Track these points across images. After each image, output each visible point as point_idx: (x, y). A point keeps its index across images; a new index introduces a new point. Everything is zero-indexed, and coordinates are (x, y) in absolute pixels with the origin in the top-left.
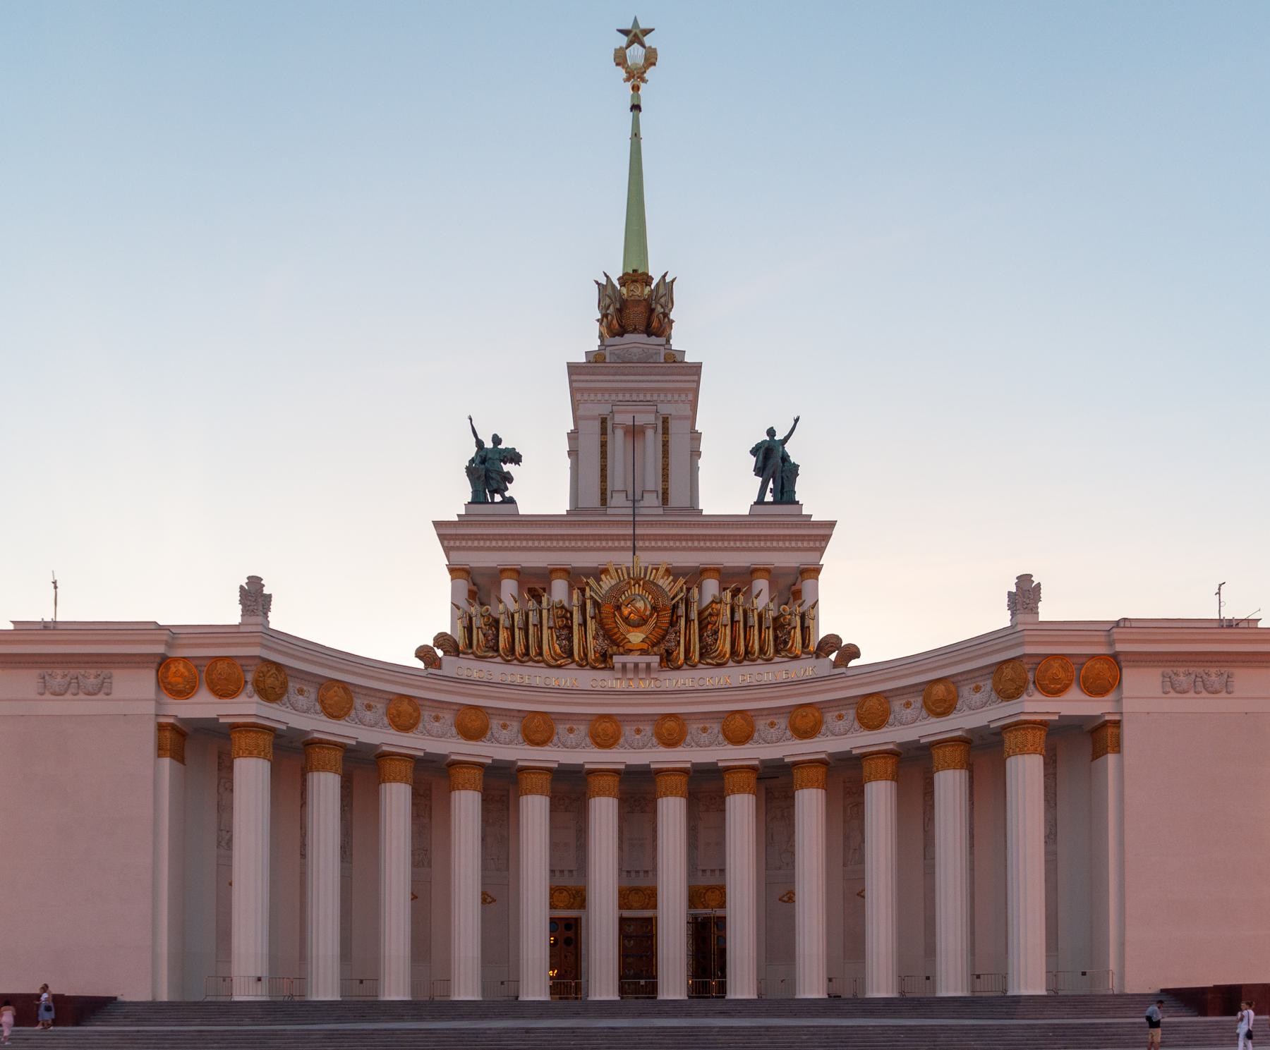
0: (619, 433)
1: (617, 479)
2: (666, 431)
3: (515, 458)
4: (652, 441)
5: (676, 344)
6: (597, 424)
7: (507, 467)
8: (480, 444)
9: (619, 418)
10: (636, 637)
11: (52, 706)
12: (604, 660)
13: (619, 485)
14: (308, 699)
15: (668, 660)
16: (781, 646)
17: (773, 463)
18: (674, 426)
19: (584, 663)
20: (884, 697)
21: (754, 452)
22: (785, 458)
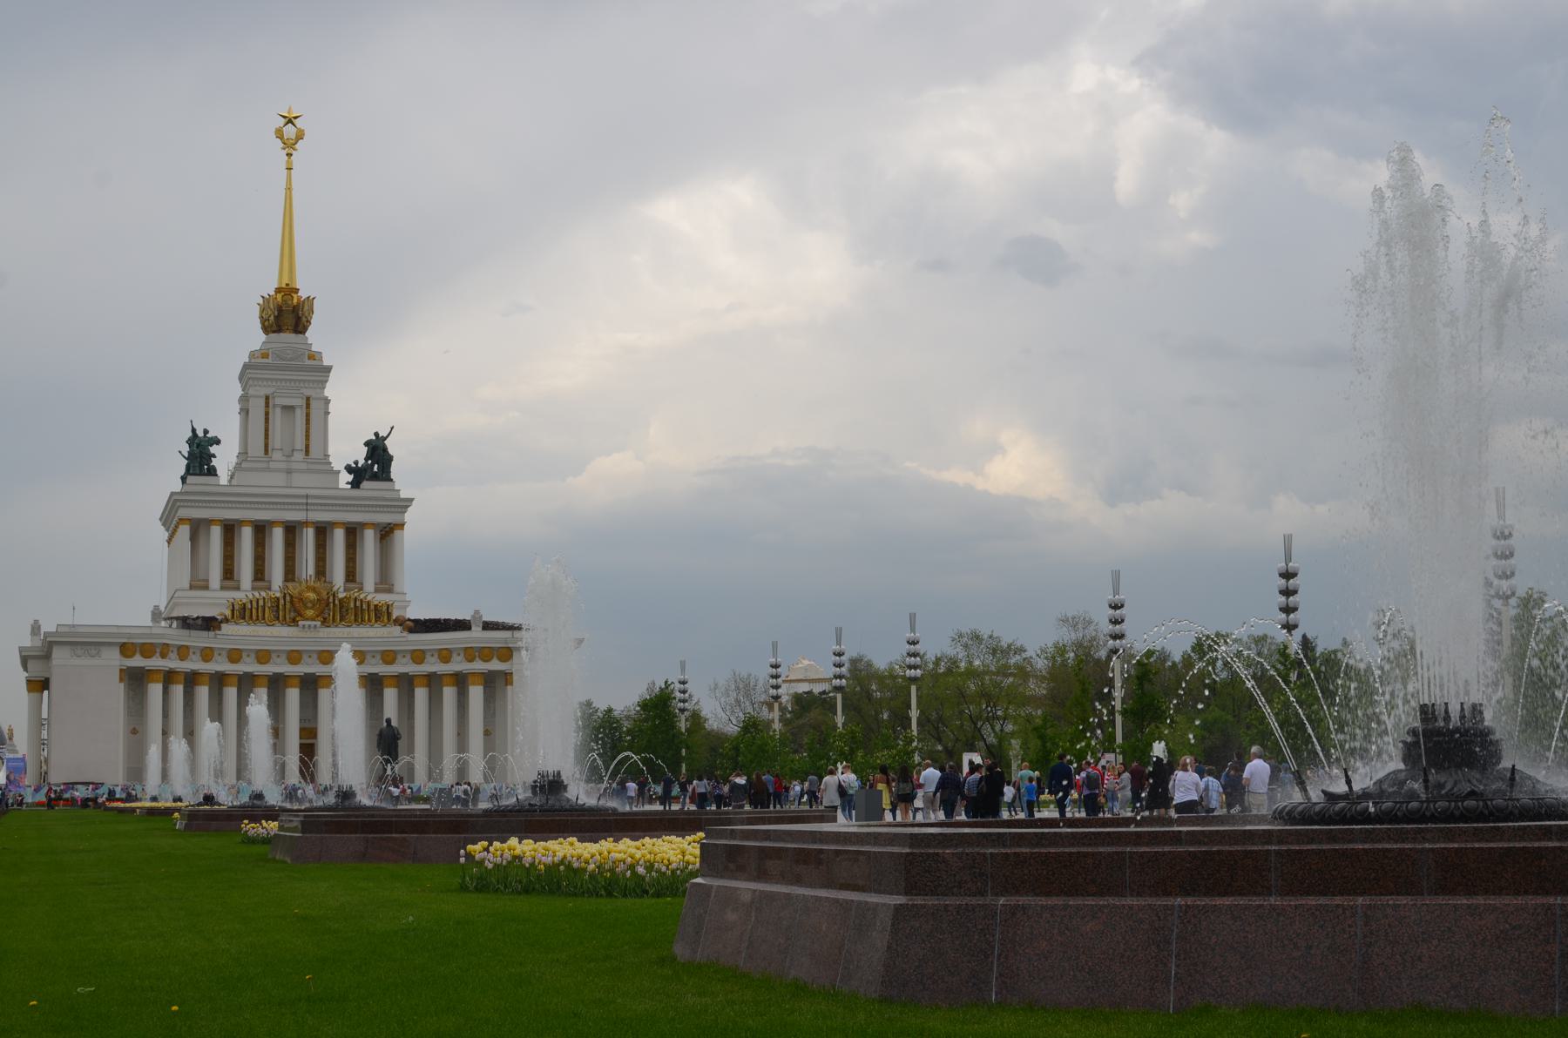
0: (278, 410)
1: (276, 440)
2: (308, 406)
3: (218, 442)
4: (300, 415)
5: (327, 392)
6: (262, 402)
7: (213, 449)
8: (194, 430)
9: (279, 401)
10: (310, 613)
11: (77, 661)
12: (294, 622)
13: (277, 445)
14: (173, 655)
15: (325, 622)
16: (378, 618)
17: (378, 451)
18: (313, 404)
19: (285, 623)
20: (423, 652)
21: (367, 444)
22: (385, 450)
